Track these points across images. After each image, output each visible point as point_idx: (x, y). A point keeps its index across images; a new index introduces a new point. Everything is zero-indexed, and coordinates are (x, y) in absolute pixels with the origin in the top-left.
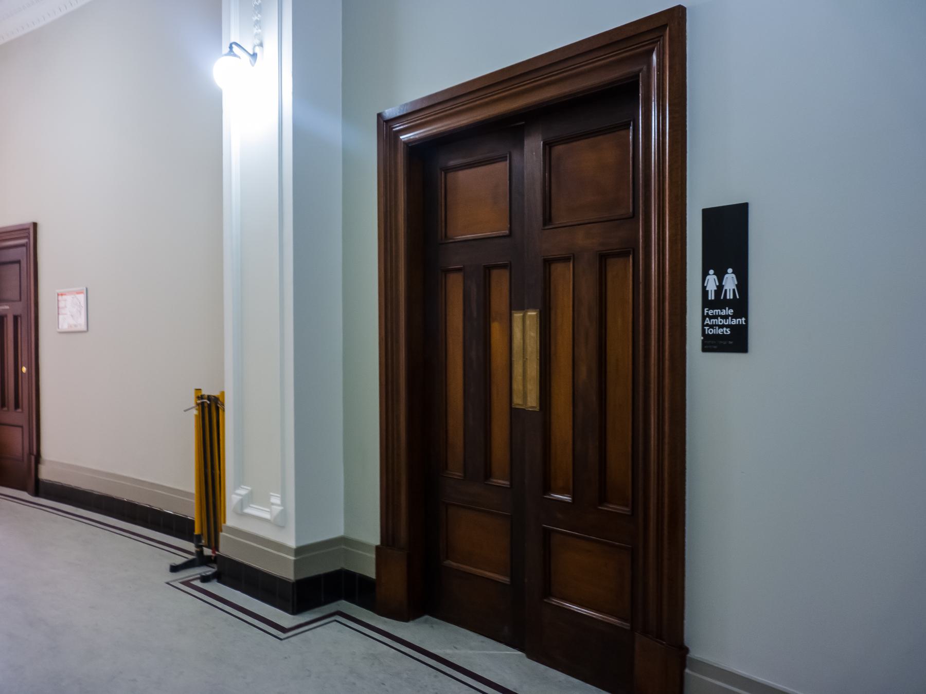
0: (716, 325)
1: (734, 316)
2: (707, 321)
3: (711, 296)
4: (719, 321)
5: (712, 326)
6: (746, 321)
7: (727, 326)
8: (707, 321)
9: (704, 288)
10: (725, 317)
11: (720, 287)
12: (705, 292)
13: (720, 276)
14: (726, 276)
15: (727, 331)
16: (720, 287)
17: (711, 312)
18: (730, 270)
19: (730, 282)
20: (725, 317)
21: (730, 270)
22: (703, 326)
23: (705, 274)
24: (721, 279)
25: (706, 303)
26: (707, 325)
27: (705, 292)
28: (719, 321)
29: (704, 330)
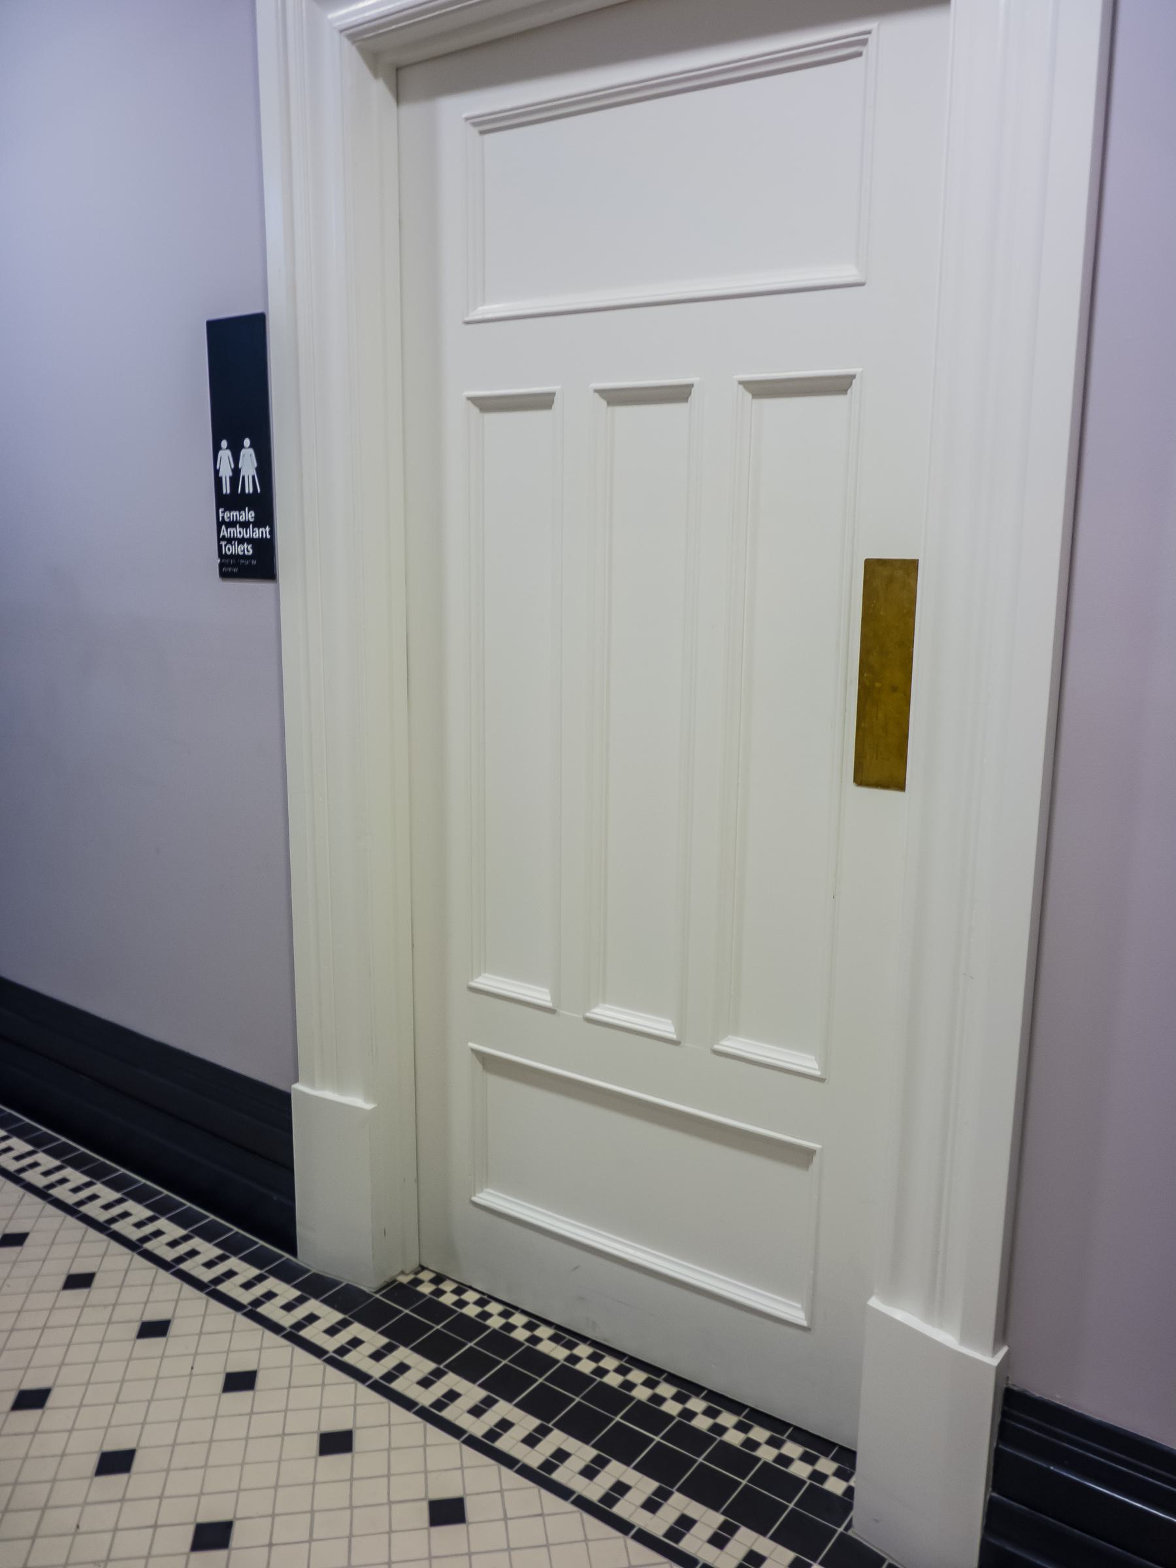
0: (235, 539)
1: (258, 523)
2: (224, 532)
3: (226, 489)
4: (238, 532)
5: (230, 541)
6: (272, 532)
7: (250, 541)
8: (224, 532)
9: (217, 472)
10: (245, 525)
12: (218, 481)
14: (243, 452)
15: (248, 550)
17: (228, 516)
18: (247, 442)
20: (245, 525)
21: (247, 442)
23: (217, 449)
24: (236, 458)
26: (224, 538)
27: (218, 481)
28: (238, 532)
29: (220, 547)
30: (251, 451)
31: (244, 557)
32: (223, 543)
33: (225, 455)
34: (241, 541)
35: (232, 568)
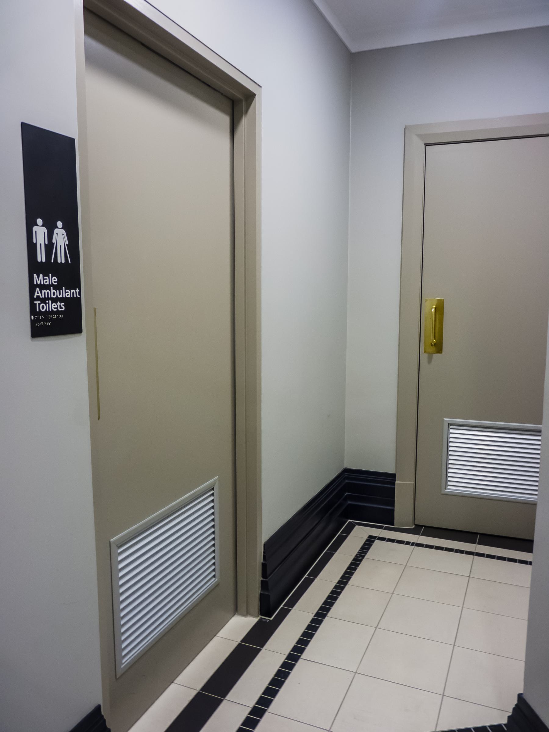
0: (48, 299)
3: (41, 257)
4: (53, 293)
5: (43, 300)
7: (61, 300)
11: (50, 247)
13: (51, 228)
14: (56, 230)
15: (61, 306)
16: (50, 247)
18: (60, 224)
19: (60, 237)
21: (60, 224)
22: (32, 299)
25: (35, 267)
26: (38, 298)
30: (63, 231)
31: (58, 312)
32: (37, 302)
33: (40, 232)
34: (55, 300)
35: (46, 326)
